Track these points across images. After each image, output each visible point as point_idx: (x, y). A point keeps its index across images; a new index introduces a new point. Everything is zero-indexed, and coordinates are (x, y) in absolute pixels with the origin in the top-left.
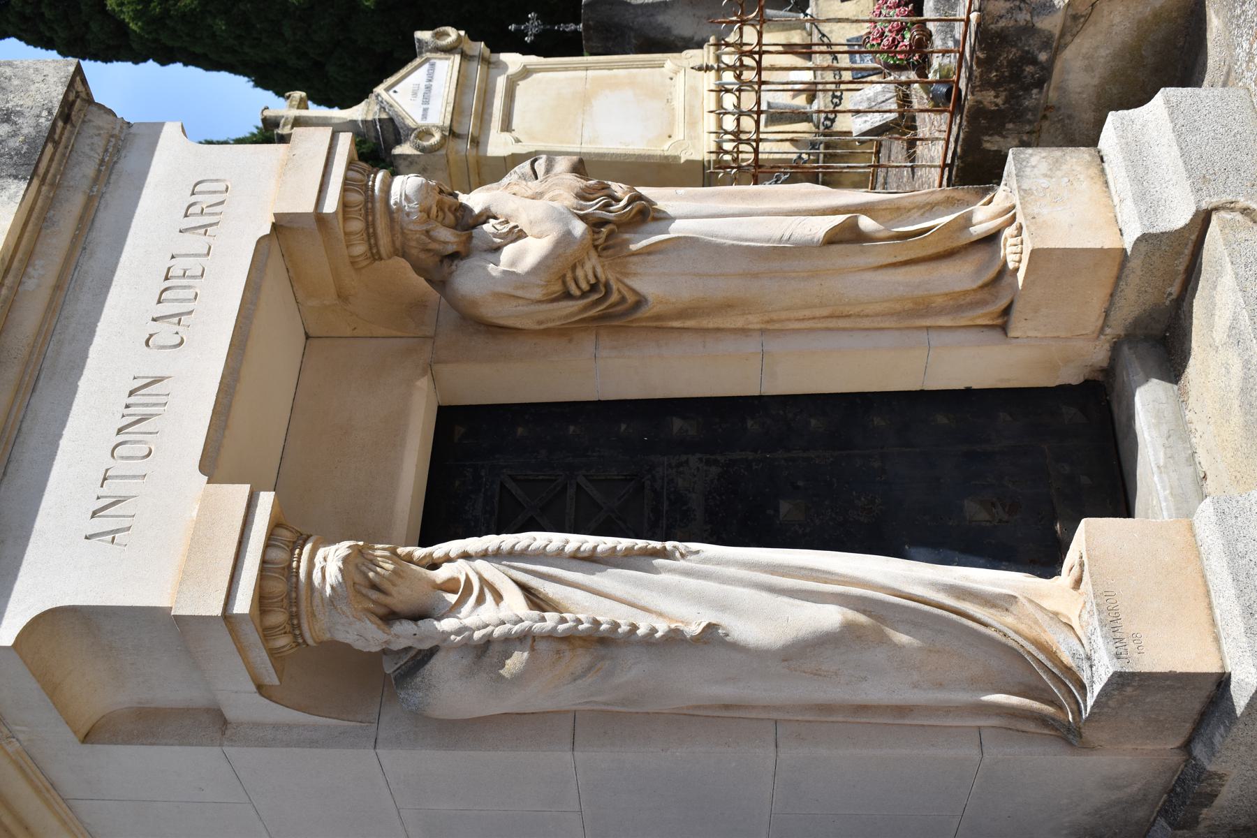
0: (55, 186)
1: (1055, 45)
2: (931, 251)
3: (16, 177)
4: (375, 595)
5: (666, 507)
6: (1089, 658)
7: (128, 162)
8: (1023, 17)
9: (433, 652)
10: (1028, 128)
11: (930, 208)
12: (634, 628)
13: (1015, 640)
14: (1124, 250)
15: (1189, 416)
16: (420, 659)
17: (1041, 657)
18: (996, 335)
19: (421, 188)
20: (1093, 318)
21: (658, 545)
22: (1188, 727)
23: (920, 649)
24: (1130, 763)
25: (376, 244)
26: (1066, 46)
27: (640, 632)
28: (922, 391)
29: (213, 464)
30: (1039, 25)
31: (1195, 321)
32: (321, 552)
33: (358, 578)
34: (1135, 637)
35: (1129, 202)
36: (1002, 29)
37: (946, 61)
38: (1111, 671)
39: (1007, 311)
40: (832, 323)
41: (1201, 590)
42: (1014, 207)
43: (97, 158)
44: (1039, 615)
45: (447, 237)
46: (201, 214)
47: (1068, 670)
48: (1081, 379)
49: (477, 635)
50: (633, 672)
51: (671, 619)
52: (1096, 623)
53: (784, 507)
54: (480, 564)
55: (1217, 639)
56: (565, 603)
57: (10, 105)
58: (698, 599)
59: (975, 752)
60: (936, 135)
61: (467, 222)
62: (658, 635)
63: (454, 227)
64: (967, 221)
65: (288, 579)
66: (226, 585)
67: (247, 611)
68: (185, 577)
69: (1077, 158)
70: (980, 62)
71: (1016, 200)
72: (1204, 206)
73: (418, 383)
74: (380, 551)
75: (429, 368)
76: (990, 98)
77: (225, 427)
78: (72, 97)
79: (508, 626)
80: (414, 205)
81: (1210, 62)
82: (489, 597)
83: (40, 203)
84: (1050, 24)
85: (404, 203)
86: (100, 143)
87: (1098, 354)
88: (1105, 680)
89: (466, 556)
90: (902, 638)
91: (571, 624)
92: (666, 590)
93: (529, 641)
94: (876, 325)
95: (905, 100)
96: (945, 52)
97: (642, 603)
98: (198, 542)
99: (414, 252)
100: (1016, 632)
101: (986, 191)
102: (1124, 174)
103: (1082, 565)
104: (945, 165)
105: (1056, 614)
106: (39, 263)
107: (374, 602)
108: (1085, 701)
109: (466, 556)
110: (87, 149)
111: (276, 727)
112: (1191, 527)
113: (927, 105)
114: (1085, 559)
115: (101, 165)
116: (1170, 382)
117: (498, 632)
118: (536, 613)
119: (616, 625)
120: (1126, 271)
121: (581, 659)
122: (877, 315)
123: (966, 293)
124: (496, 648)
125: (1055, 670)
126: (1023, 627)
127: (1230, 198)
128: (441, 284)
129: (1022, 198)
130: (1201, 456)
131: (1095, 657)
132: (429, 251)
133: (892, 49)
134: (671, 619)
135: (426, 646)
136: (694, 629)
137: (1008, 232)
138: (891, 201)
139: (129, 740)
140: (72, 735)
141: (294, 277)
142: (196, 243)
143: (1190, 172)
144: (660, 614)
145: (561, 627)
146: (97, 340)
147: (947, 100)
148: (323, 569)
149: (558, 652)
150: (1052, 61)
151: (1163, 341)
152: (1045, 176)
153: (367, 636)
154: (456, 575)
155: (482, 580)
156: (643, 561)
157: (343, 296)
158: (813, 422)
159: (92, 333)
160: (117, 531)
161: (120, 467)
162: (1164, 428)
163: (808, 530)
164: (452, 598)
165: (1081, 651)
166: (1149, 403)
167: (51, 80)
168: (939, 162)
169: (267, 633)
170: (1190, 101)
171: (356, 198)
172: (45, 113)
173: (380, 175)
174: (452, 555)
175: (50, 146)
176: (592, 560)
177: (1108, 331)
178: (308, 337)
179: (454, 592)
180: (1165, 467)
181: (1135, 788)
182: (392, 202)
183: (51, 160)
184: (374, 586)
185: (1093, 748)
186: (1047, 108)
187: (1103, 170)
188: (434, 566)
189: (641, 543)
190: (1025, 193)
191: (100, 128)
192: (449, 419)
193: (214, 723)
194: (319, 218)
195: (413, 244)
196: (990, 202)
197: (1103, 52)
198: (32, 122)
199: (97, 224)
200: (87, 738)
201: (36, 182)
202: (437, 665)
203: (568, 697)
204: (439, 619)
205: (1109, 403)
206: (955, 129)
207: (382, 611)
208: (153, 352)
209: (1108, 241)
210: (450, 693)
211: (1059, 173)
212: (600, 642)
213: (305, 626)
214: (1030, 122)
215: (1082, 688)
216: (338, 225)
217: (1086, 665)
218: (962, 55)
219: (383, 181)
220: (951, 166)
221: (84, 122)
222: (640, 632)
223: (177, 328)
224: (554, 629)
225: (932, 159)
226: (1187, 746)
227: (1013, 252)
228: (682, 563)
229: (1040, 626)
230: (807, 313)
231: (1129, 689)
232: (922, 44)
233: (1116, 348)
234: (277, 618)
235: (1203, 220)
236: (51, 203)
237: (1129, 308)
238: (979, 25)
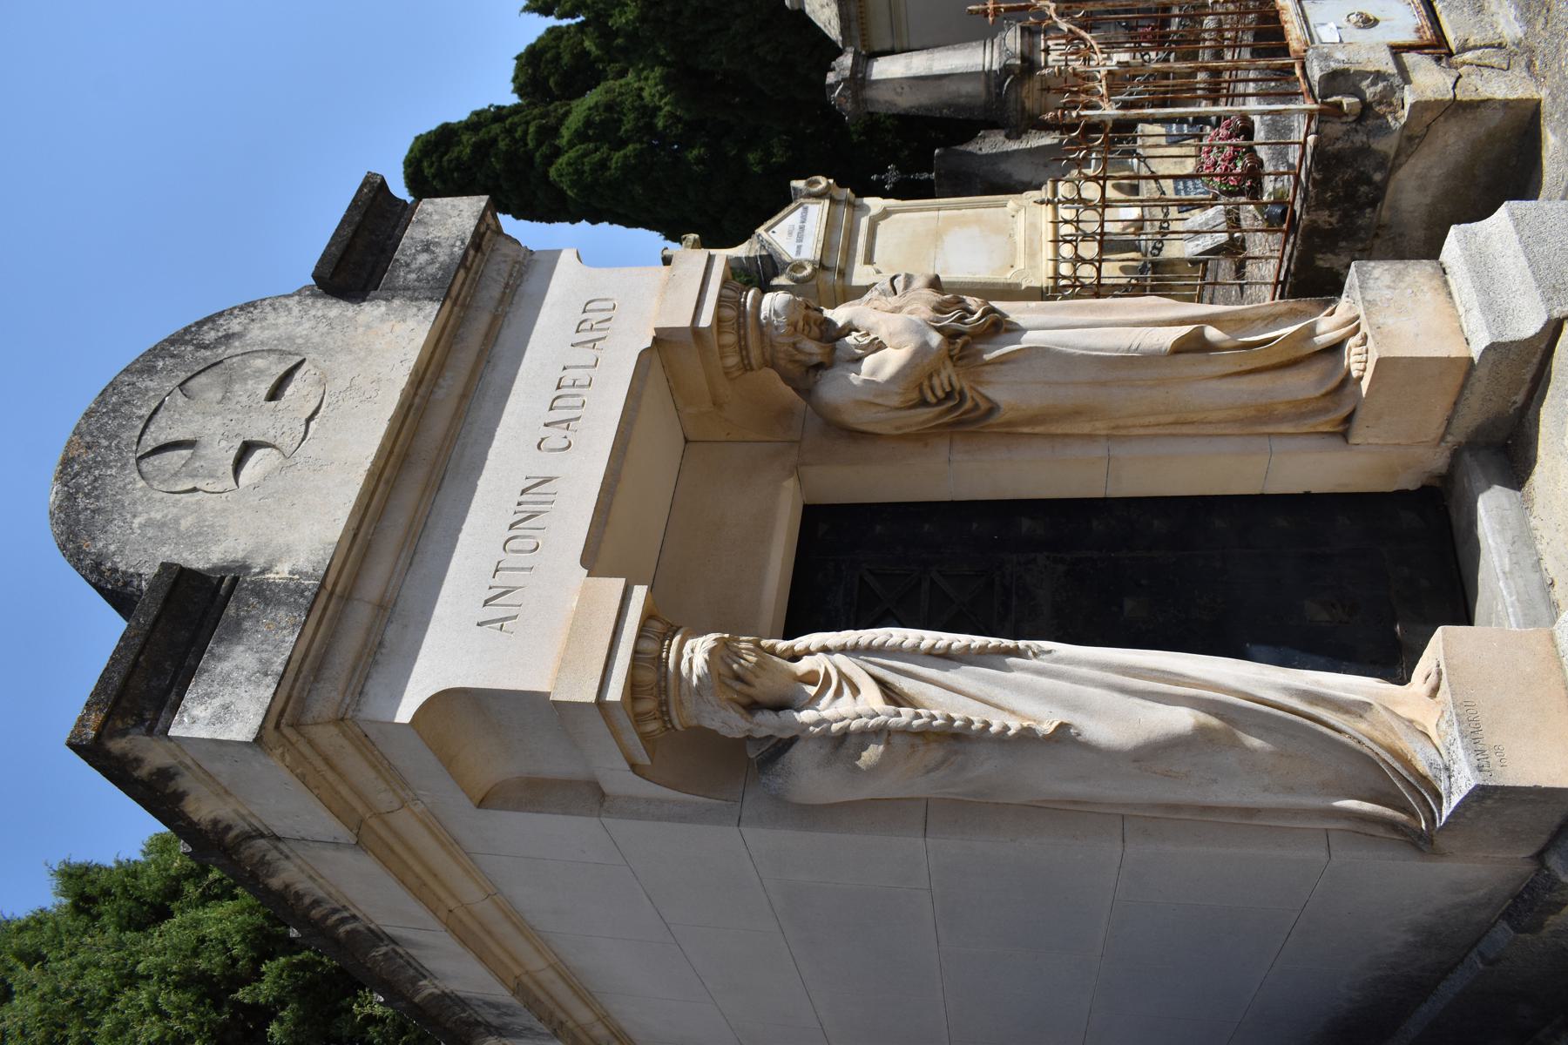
0: (466, 307)
1: (1388, 166)
2: (1275, 360)
3: (431, 299)
4: (739, 686)
6: (1447, 769)
7: (530, 286)
8: (1359, 139)
9: (793, 741)
10: (1360, 246)
11: (1274, 320)
12: (987, 725)
13: (1369, 747)
14: (1471, 359)
15: (1534, 522)
16: (780, 747)
17: (1397, 765)
18: (1337, 442)
19: (788, 303)
20: (1435, 425)
21: (1010, 643)
22: (1544, 838)
23: (1272, 753)
24: (1480, 871)
25: (748, 357)
26: (1400, 166)
27: (993, 729)
28: (1262, 495)
29: (594, 559)
30: (1375, 146)
31: (1542, 429)
32: (689, 644)
33: (723, 670)
34: (1497, 750)
35: (1476, 312)
36: (1339, 150)
37: (1279, 185)
38: (1473, 784)
39: (1348, 419)
40: (1171, 430)
42: (1358, 317)
43: (503, 281)
44: (1395, 723)
45: (813, 349)
46: (591, 329)
47: (1423, 778)
48: (1419, 485)
49: (835, 727)
50: (985, 767)
51: (1024, 717)
52: (1457, 734)
53: (1129, 604)
54: (839, 659)
56: (920, 698)
58: (1049, 698)
59: (1324, 854)
60: (1268, 256)
61: (832, 335)
62: (1011, 733)
63: (819, 340)
64: (1311, 332)
65: (658, 669)
66: (600, 673)
67: (618, 698)
68: (564, 663)
69: (1418, 272)
70: (1315, 183)
71: (1360, 310)
72: (1556, 314)
74: (745, 643)
75: (796, 470)
76: (1324, 218)
77: (606, 523)
78: (483, 229)
79: (864, 720)
81: (1546, 179)
82: (847, 690)
83: (451, 322)
84: (1387, 145)
86: (505, 268)
87: (1438, 460)
88: (1465, 791)
89: (826, 650)
90: (1254, 742)
91: (925, 720)
92: (1019, 688)
93: (885, 736)
94: (1219, 431)
95: (1234, 222)
96: (1278, 175)
97: (995, 700)
98: (577, 633)
99: (782, 363)
100: (1371, 740)
101: (1328, 303)
102: (1469, 284)
103: (1439, 673)
104: (1278, 282)
105: (1411, 721)
106: (448, 374)
107: (738, 692)
108: (1440, 811)
109: (826, 650)
110: (494, 275)
111: (649, 801)
112: (1552, 638)
113: (1259, 224)
114: (1442, 667)
116: (1513, 488)
117: (855, 725)
118: (891, 708)
119: (969, 722)
120: (1473, 380)
121: (936, 753)
122: (1220, 422)
123: (1308, 401)
124: (853, 740)
125: (1411, 779)
126: (1376, 734)
128: (806, 392)
129: (1366, 310)
130: (1548, 563)
131: (1455, 768)
132: (796, 362)
133: (1225, 175)
134: (1024, 717)
135: (787, 735)
136: (1047, 728)
137: (1352, 342)
138: (1236, 312)
139: (519, 806)
140: (467, 801)
141: (676, 388)
142: (586, 355)
143: (1540, 282)
144: (1013, 712)
145: (916, 723)
146: (495, 443)
147: (1279, 219)
148: (690, 660)
149: (912, 746)
150: (1386, 181)
151: (1508, 450)
152: (1389, 287)
153: (733, 724)
154: (815, 668)
155: (840, 673)
156: (996, 659)
157: (717, 404)
158: (1156, 522)
159: (492, 437)
160: (506, 619)
161: (511, 560)
162: (1509, 534)
164: (812, 690)
165: (1439, 761)
166: (1492, 510)
167: (465, 214)
168: (1273, 280)
169: (638, 719)
171: (729, 313)
173: (751, 293)
174: (812, 648)
175: (462, 272)
176: (946, 657)
177: (1449, 438)
178: (686, 441)
179: (814, 684)
180: (1511, 572)
181: (1481, 892)
183: (463, 284)
184: (738, 677)
185: (1443, 855)
186: (1380, 227)
187: (1446, 282)
188: (795, 657)
189: (994, 641)
190: (1369, 304)
191: (506, 255)
192: (815, 518)
193: (591, 796)
194: (695, 331)
195: (781, 355)
196: (1332, 313)
197: (1436, 172)
198: (448, 251)
200: (482, 804)
201: (448, 303)
202: (797, 754)
203: (921, 787)
204: (799, 710)
205: (1446, 508)
206: (1288, 248)
207: (745, 700)
208: (544, 454)
209: (1455, 350)
210: (810, 779)
211: (1403, 285)
212: (954, 739)
213: (673, 714)
214: (1362, 240)
215: (1438, 797)
216: (713, 338)
217: (1444, 776)
218: (1297, 177)
219: (754, 298)
220: (1283, 283)
222: (993, 729)
223: (566, 433)
224: (909, 724)
225: (1263, 277)
226: (1540, 857)
227: (1359, 362)
228: (1034, 662)
229: (1395, 734)
230: (1152, 420)
231: (1489, 802)
232: (1255, 172)
233: (1456, 455)
234: (648, 705)
235: (1553, 329)
236: (461, 322)
237: (1473, 415)
238: (1315, 147)
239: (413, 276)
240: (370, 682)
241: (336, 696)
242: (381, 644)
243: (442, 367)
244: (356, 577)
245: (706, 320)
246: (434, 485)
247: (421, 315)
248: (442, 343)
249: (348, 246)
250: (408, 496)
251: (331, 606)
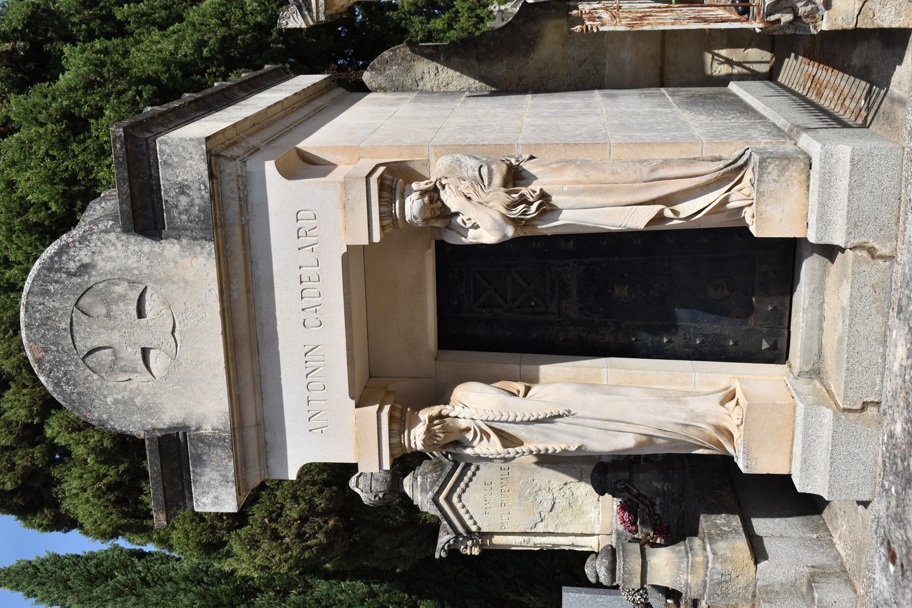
0: (223, 226)
5: (557, 289)
12: (547, 450)
32: (413, 431)
41: (790, 438)
55: (791, 460)
57: (180, 179)
71: (754, 195)
80: (419, 220)
82: (485, 438)
86: (233, 185)
106: (234, 280)
115: (240, 201)
127: (865, 240)
129: (758, 199)
146: (279, 323)
152: (775, 181)
170: (865, 160)
172: (202, 187)
191: (230, 174)
199: (253, 244)
211: (783, 179)
221: (220, 172)
222: (550, 452)
223: (316, 315)
239: (184, 217)
240: (270, 462)
241: (257, 472)
242: (266, 442)
243: (228, 276)
244: (241, 415)
245: (377, 238)
246: (256, 352)
247: (205, 252)
248: (222, 258)
249: (132, 199)
250: (246, 364)
251: (237, 434)
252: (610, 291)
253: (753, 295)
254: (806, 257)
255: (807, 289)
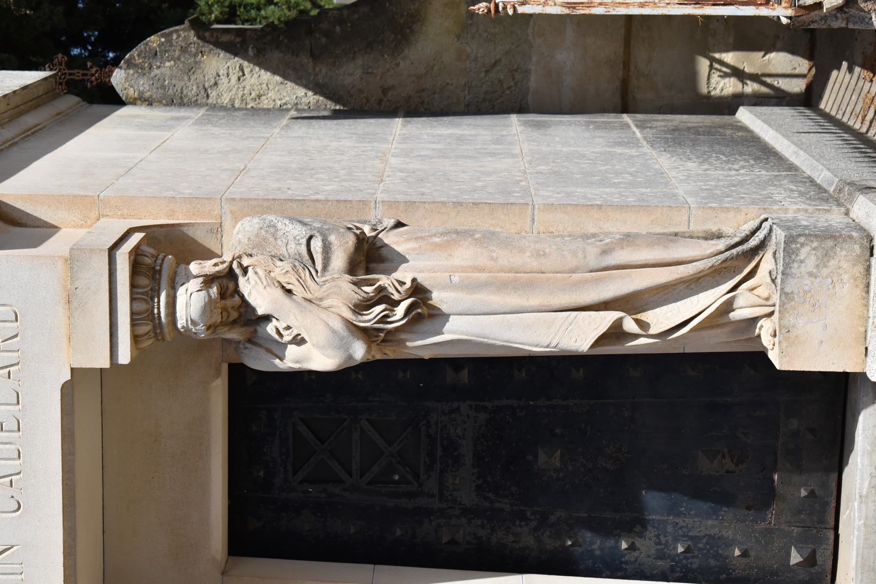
5: (439, 452)
71: (776, 298)
73: (214, 384)
80: (201, 327)
85: (190, 327)
129: (783, 304)
152: (811, 274)
163: (561, 475)
180: (867, 497)
182: (179, 326)
211: (825, 272)
245: (124, 356)
252: (530, 457)
253: (774, 469)
254: (866, 406)
255: (866, 462)
